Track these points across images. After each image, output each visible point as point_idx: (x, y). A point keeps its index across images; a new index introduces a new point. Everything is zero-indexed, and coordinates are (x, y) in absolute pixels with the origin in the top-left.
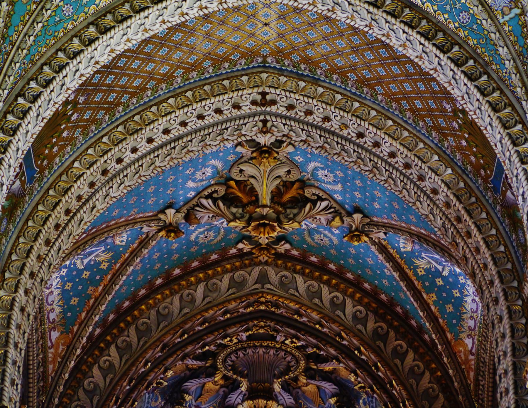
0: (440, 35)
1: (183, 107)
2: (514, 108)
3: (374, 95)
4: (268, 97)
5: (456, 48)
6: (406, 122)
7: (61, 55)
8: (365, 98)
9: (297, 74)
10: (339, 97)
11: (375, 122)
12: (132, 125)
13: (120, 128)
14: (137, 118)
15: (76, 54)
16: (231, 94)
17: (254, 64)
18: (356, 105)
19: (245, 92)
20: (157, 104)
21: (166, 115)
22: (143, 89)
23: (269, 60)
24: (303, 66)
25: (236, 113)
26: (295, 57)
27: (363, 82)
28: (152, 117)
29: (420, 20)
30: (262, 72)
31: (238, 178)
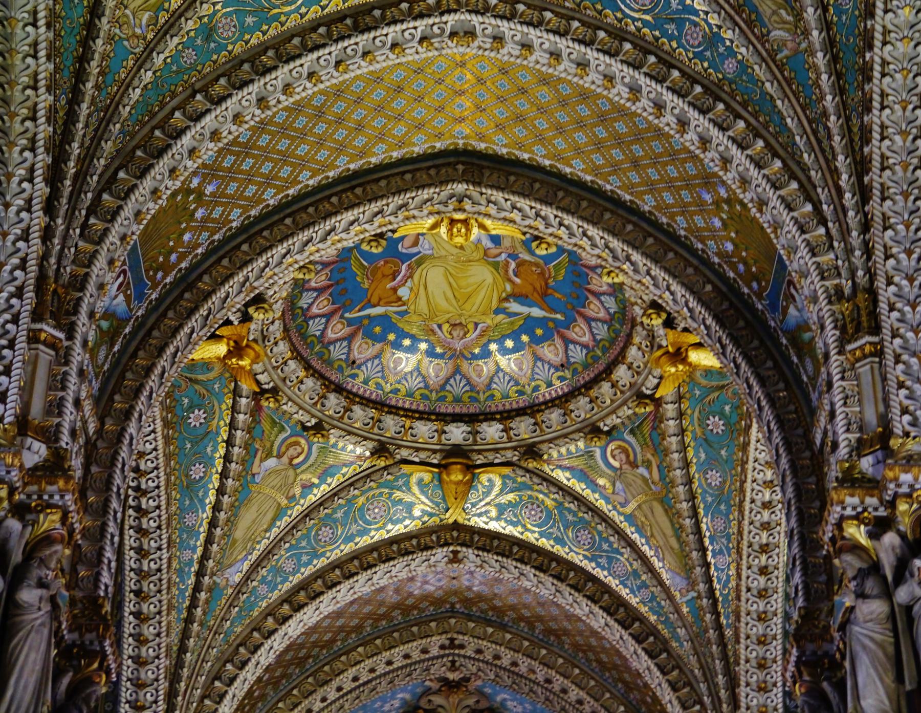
0: (622, 610)
1: (372, 656)
2: (692, 688)
3: (561, 644)
4: (457, 642)
5: (637, 624)
6: (592, 670)
7: (256, 634)
8: (552, 645)
9: (485, 619)
10: (526, 643)
11: (562, 670)
12: (322, 676)
13: (310, 680)
14: (326, 668)
15: (272, 633)
16: (420, 642)
17: (443, 609)
18: (544, 652)
19: (434, 638)
20: (347, 653)
21: (355, 664)
22: (333, 641)
23: (458, 606)
24: (490, 613)
25: (423, 656)
26: (484, 606)
27: (548, 632)
28: (341, 667)
29: (603, 593)
30: (450, 617)
31: (427, 707)
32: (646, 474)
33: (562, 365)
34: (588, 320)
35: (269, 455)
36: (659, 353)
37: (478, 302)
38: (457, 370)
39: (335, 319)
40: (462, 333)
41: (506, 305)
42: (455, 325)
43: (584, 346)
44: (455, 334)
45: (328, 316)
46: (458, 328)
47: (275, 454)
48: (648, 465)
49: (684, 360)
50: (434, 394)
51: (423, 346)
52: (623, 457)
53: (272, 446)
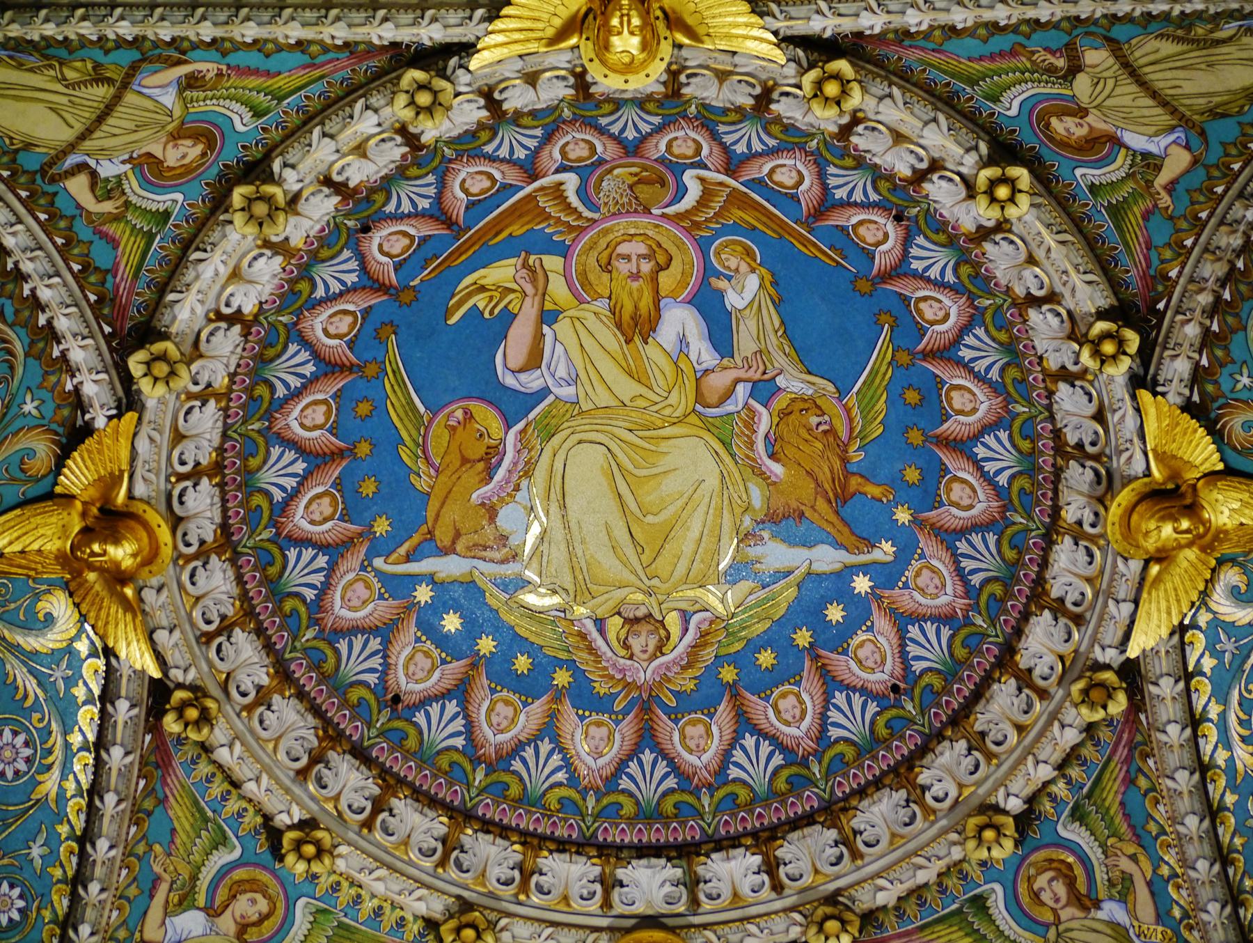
32: (1121, 916)
33: (895, 688)
34: (949, 537)
35: (185, 902)
36: (1125, 497)
37: (688, 548)
38: (647, 738)
39: (353, 561)
40: (653, 643)
41: (753, 552)
42: (637, 620)
43: (943, 619)
44: (636, 644)
45: (335, 550)
46: (644, 628)
47: (201, 900)
48: (1123, 889)
49: (1192, 509)
50: (591, 801)
51: (562, 678)
52: (1060, 888)
53: (194, 878)
